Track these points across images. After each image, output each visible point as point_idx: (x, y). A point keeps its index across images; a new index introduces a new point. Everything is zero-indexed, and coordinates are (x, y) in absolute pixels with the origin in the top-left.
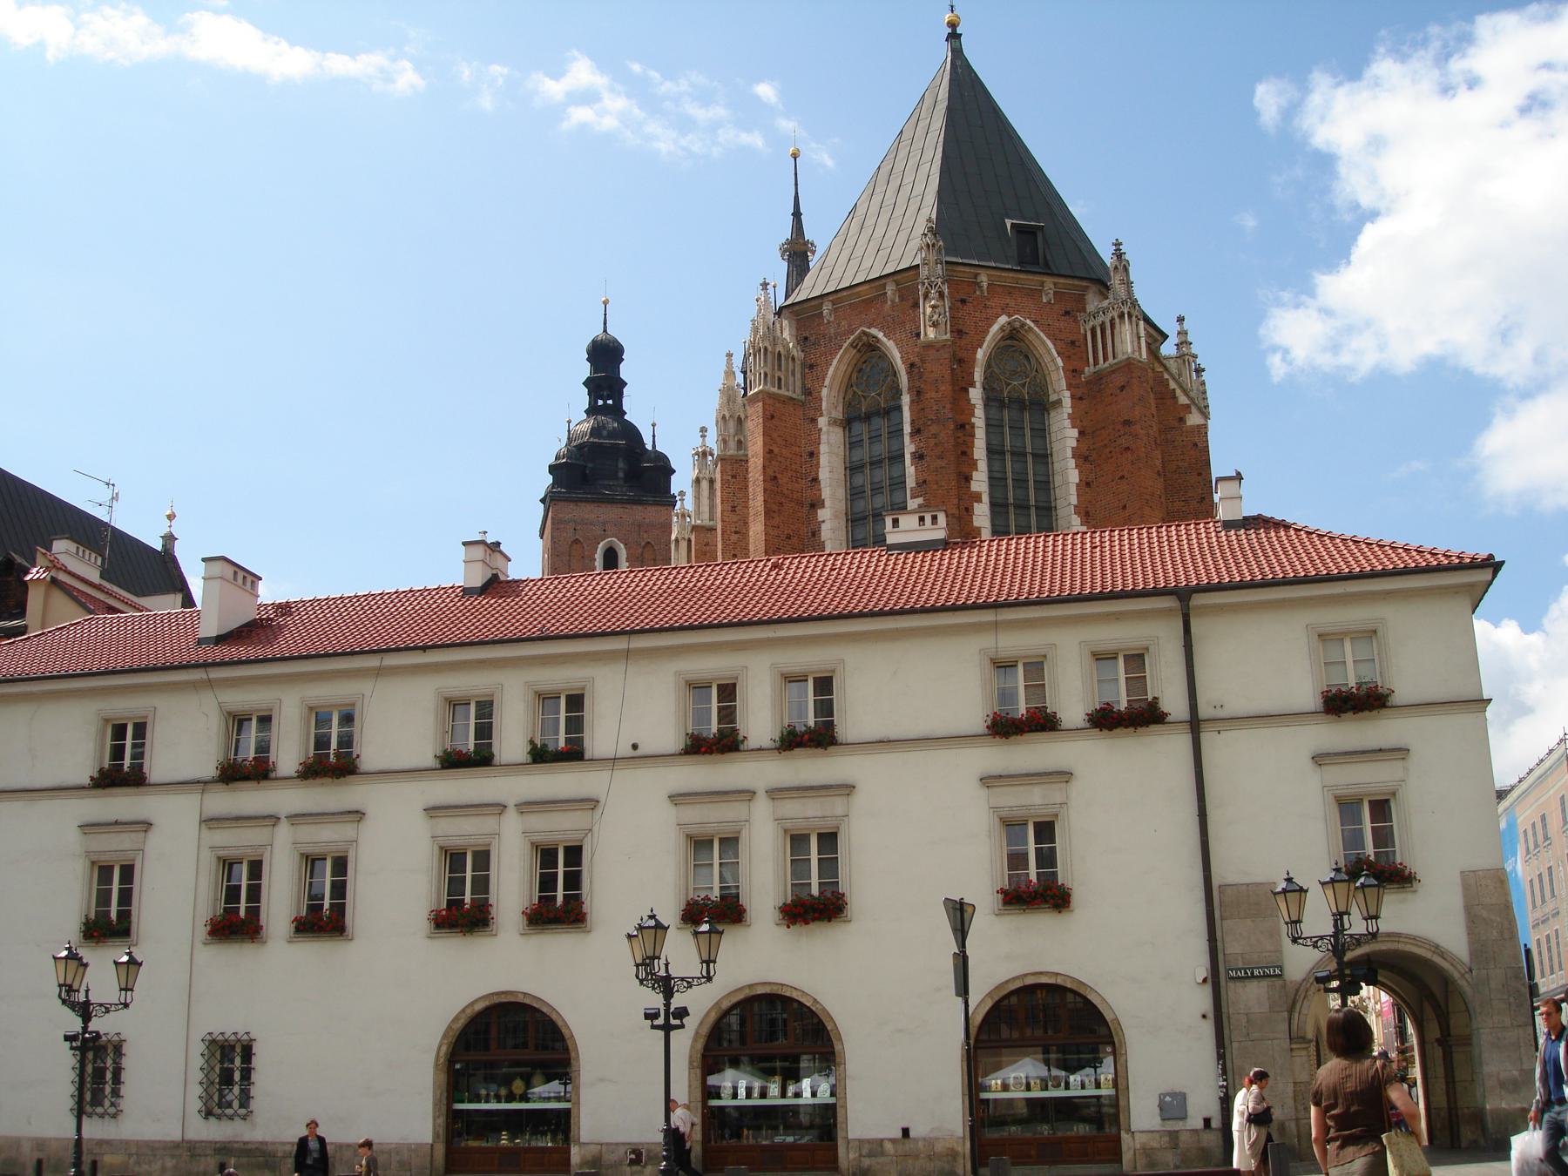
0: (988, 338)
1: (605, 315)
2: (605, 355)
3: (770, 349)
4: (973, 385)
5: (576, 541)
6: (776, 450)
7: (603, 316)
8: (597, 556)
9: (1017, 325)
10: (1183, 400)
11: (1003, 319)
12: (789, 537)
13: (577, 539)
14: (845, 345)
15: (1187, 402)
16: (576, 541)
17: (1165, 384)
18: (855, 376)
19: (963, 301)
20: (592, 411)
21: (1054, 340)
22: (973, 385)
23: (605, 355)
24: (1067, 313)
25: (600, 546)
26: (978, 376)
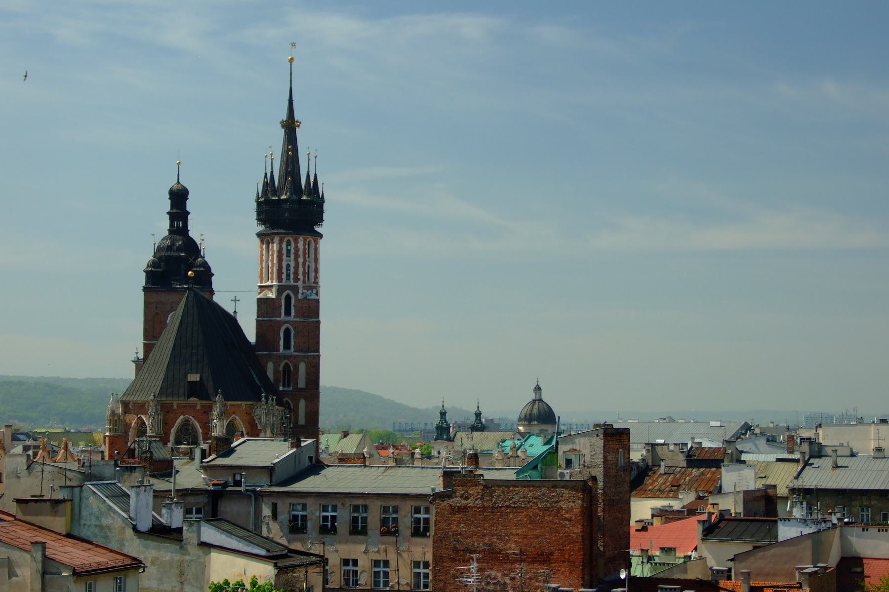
0: (176, 424)
3: (112, 419)
4: (169, 441)
5: (157, 314)
7: (177, 177)
9: (187, 418)
10: (259, 428)
15: (260, 428)
19: (168, 412)
21: (199, 422)
22: (169, 441)
24: (205, 412)
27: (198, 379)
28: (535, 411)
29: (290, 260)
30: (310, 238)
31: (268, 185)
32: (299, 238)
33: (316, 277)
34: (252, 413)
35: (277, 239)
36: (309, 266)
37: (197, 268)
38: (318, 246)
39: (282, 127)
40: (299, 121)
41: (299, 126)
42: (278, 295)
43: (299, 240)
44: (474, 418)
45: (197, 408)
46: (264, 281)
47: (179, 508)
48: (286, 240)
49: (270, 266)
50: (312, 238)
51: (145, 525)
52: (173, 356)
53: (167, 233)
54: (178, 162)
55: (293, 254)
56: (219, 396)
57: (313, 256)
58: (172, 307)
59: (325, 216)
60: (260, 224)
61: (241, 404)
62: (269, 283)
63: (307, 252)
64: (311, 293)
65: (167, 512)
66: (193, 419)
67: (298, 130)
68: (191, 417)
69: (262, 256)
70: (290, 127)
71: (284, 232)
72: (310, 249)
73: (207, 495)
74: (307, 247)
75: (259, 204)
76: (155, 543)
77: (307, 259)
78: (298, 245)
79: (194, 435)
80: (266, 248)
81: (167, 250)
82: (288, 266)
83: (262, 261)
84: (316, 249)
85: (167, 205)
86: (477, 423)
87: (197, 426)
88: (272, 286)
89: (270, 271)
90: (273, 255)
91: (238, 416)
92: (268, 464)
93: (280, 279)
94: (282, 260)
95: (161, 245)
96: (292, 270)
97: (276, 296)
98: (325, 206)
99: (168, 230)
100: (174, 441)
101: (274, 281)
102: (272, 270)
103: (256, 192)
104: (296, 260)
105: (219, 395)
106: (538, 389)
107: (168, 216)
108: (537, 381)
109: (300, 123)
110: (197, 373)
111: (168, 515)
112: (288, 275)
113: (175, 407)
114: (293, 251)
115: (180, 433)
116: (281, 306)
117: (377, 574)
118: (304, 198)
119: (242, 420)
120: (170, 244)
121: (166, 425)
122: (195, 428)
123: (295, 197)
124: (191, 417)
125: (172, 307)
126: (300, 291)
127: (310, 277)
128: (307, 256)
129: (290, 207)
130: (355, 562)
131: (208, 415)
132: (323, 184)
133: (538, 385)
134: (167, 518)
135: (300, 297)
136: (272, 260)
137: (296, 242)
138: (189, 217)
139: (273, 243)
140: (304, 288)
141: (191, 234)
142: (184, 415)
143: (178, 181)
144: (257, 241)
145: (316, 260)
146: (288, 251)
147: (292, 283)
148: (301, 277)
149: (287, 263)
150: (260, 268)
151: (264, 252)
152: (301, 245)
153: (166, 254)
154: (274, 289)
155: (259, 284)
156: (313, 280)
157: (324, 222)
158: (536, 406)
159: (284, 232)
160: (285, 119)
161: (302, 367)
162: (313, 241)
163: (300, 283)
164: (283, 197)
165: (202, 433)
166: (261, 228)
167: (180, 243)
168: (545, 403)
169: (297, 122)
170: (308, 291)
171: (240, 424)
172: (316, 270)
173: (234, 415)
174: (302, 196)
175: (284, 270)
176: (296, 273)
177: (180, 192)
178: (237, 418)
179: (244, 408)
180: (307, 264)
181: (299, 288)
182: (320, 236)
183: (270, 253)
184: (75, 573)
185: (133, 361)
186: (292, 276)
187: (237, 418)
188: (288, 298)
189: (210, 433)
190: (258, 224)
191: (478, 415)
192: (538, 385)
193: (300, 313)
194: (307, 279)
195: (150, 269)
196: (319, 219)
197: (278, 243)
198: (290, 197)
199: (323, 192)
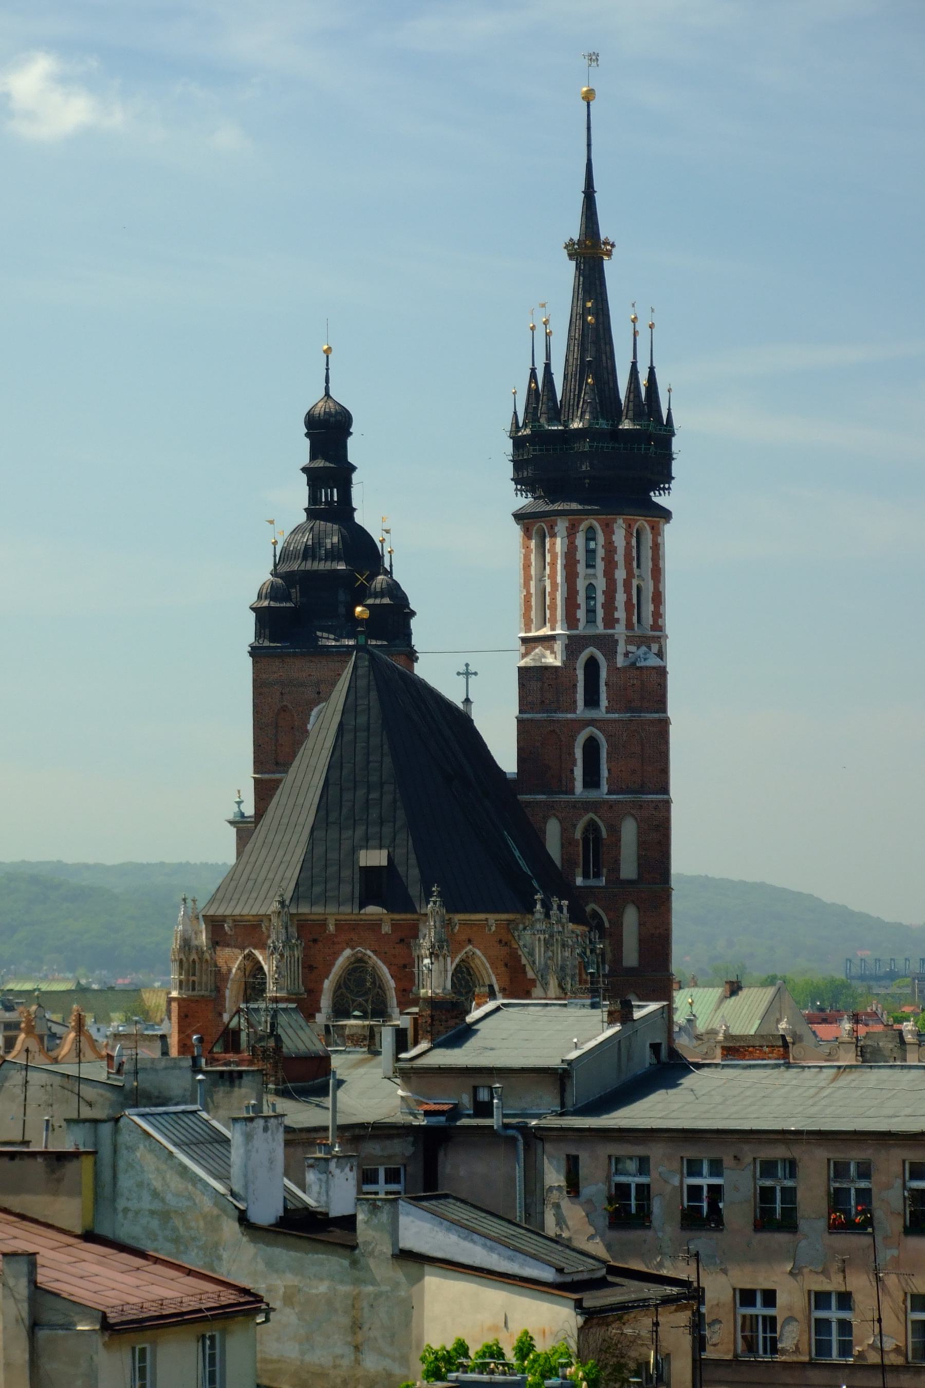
1: (327, 369)
3: (184, 959)
5: (284, 709)
9: (360, 955)
10: (531, 974)
11: (348, 952)
13: (286, 706)
16: (284, 709)
17: (518, 959)
19: (315, 941)
20: (312, 513)
21: (389, 965)
22: (319, 1010)
24: (402, 941)
27: (384, 863)
29: (594, 575)
30: (642, 522)
32: (615, 521)
33: (658, 615)
34: (513, 942)
35: (562, 526)
36: (639, 589)
37: (376, 598)
38: (660, 540)
39: (571, 256)
40: (611, 240)
41: (609, 254)
43: (615, 526)
45: (383, 933)
46: (533, 626)
47: (347, 1169)
48: (583, 526)
49: (548, 589)
50: (646, 521)
52: (324, 806)
53: (302, 517)
54: (325, 347)
55: (603, 559)
56: (435, 903)
57: (650, 564)
58: (319, 693)
59: (676, 468)
60: (521, 490)
61: (487, 920)
62: (546, 631)
63: (634, 554)
64: (645, 654)
65: (320, 1180)
66: (374, 957)
67: (608, 264)
68: (369, 952)
69: (527, 566)
71: (580, 507)
72: (642, 548)
73: (411, 1139)
74: (634, 542)
75: (519, 443)
76: (292, 1254)
77: (636, 571)
78: (614, 538)
79: (378, 994)
81: (305, 558)
82: (591, 588)
84: (657, 548)
88: (552, 638)
89: (548, 602)
90: (553, 564)
91: (479, 949)
92: (554, 1062)
93: (571, 621)
96: (600, 598)
97: (564, 662)
98: (677, 444)
99: (306, 510)
100: (330, 1010)
101: (559, 624)
102: (553, 599)
104: (609, 574)
107: (304, 478)
109: (613, 246)
110: (381, 848)
112: (591, 611)
113: (332, 928)
114: (601, 553)
115: (344, 990)
116: (575, 686)
117: (822, 1326)
118: (626, 425)
119: (489, 958)
120: (310, 543)
122: (379, 977)
123: (603, 424)
125: (319, 693)
126: (621, 648)
127: (643, 615)
128: (635, 564)
130: (770, 1297)
131: (409, 947)
132: (669, 391)
134: (319, 1193)
135: (620, 661)
137: (609, 530)
138: (355, 477)
139: (553, 535)
140: (629, 640)
141: (358, 518)
142: (353, 948)
143: (327, 394)
144: (516, 530)
145: (657, 573)
146: (591, 553)
147: (600, 629)
148: (621, 614)
149: (587, 582)
151: (533, 557)
152: (619, 538)
153: (302, 568)
154: (558, 646)
155: (523, 635)
157: (673, 482)
159: (580, 507)
160: (576, 238)
161: (629, 831)
162: (648, 528)
163: (620, 630)
164: (576, 425)
166: (523, 501)
167: (335, 540)
170: (638, 648)
171: (486, 969)
172: (658, 598)
173: (470, 947)
174: (620, 421)
175: (581, 599)
176: (610, 605)
177: (332, 419)
178: (478, 952)
179: (493, 928)
180: (635, 582)
181: (617, 640)
182: (666, 515)
183: (548, 559)
184: (106, 1325)
185: (232, 823)
186: (600, 613)
187: (478, 952)
188: (592, 666)
189: (414, 989)
190: (516, 489)
194: (635, 618)
197: (565, 534)
198: (591, 424)
199: (669, 409)
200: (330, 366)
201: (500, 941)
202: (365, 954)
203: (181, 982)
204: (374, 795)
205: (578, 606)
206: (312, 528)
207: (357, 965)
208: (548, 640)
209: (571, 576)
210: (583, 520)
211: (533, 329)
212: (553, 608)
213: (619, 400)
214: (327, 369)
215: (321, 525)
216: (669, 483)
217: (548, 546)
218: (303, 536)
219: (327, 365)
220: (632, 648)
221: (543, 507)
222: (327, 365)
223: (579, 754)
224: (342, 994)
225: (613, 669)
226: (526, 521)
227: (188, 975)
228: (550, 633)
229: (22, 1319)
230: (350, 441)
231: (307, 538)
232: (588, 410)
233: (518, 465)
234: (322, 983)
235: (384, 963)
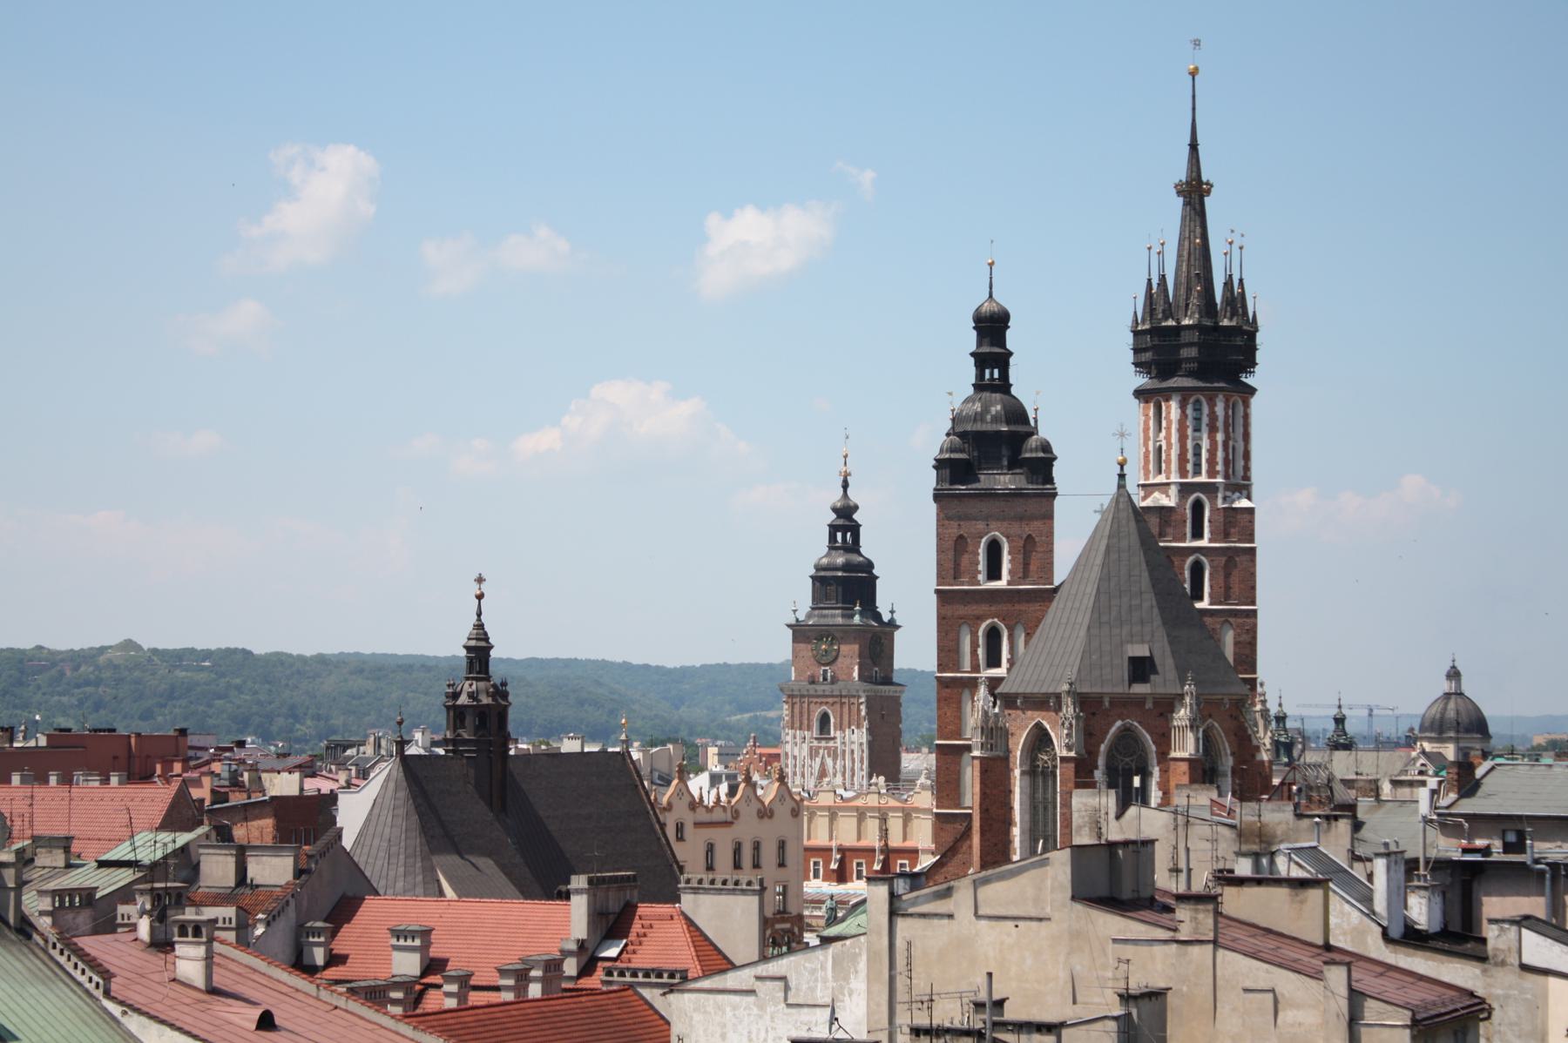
0: (1109, 737)
1: (991, 278)
2: (992, 326)
3: (985, 727)
4: (1097, 768)
6: (988, 791)
7: (988, 289)
8: (980, 551)
9: (1128, 725)
11: (1119, 723)
12: (996, 845)
14: (1030, 726)
18: (1037, 743)
19: (1094, 714)
20: (979, 387)
22: (1097, 768)
23: (992, 326)
24: (1161, 714)
25: (984, 540)
26: (1101, 761)
27: (1148, 654)
28: (1451, 714)
30: (1236, 398)
31: (1155, 300)
32: (1217, 396)
33: (1247, 468)
34: (1241, 717)
36: (1234, 448)
39: (1179, 193)
41: (1208, 192)
42: (1180, 500)
43: (1217, 400)
44: (1331, 726)
45: (1147, 707)
46: (1151, 476)
47: (1436, 895)
48: (1191, 400)
49: (1164, 448)
50: (1240, 397)
51: (1396, 932)
52: (1097, 608)
53: (971, 391)
54: (990, 261)
55: (1207, 425)
56: (1190, 685)
59: (1260, 356)
60: (1141, 372)
61: (1222, 699)
62: (1161, 479)
63: (1231, 421)
65: (1420, 903)
66: (1140, 727)
67: (1207, 200)
68: (1136, 724)
69: (1146, 430)
70: (1194, 192)
71: (1201, 384)
73: (1449, 871)
74: (1230, 412)
75: (1136, 333)
76: (1430, 963)
77: (1232, 435)
78: (1217, 409)
79: (1141, 755)
80: (1154, 413)
81: (975, 420)
83: (1146, 439)
84: (1246, 417)
85: (970, 340)
86: (1338, 736)
87: (1147, 740)
88: (1168, 484)
90: (1169, 428)
91: (1217, 722)
93: (1183, 472)
94: (1186, 437)
95: (962, 411)
97: (1177, 504)
98: (1259, 338)
100: (1104, 768)
102: (1168, 455)
103: (1132, 313)
105: (1189, 682)
106: (1454, 674)
108: (1451, 659)
109: (1212, 186)
110: (1143, 642)
111: (1421, 909)
112: (1197, 466)
113: (1107, 704)
114: (1205, 420)
115: (1114, 752)
116: (1185, 521)
118: (1226, 322)
120: (979, 409)
121: (1089, 735)
122: (1143, 743)
123: (1208, 323)
124: (1136, 724)
129: (1199, 339)
133: (1454, 667)
136: (1168, 438)
137: (1212, 405)
138: (1012, 360)
141: (1014, 391)
142: (1123, 720)
143: (991, 296)
145: (1246, 436)
147: (1203, 478)
149: (1195, 442)
150: (1144, 453)
151: (1151, 423)
152: (1220, 409)
153: (974, 429)
154: (1173, 490)
155: (1142, 482)
156: (1242, 474)
157: (1257, 367)
158: (1452, 705)
159: (1201, 384)
160: (1184, 180)
162: (1240, 403)
163: (1219, 480)
164: (1186, 322)
165: (1156, 752)
166: (1141, 381)
167: (999, 407)
168: (1468, 698)
169: (1207, 184)
171: (1221, 737)
172: (1247, 456)
173: (1210, 720)
175: (1190, 456)
178: (1216, 725)
180: (1231, 443)
182: (1251, 391)
183: (1164, 424)
184: (1415, 1023)
185: (899, 627)
187: (1216, 725)
190: (1136, 371)
191: (1340, 721)
192: (1454, 667)
193: (1223, 533)
194: (1231, 471)
195: (947, 456)
196: (1249, 363)
198: (1199, 321)
199: (1254, 312)
200: (993, 276)
201: (1231, 716)
202: (1132, 725)
203: (982, 744)
204: (1135, 602)
205: (1188, 461)
206: (980, 399)
207: (1125, 733)
208: (1163, 487)
209: (1183, 438)
210: (1192, 395)
211: (1149, 248)
212: (1168, 462)
213: (1216, 304)
214: (991, 278)
215: (986, 395)
216: (1254, 367)
217: (1164, 415)
218: (974, 404)
219: (991, 274)
220: (1229, 494)
221: (1157, 384)
222: (991, 274)
223: (1187, 574)
224: (1113, 755)
225: (1214, 510)
226: (1146, 395)
227: (987, 738)
228: (1165, 481)
229: (1343, 1015)
230: (1008, 333)
231: (978, 407)
232: (1197, 311)
233: (1137, 351)
234: (1099, 746)
235: (1147, 732)
